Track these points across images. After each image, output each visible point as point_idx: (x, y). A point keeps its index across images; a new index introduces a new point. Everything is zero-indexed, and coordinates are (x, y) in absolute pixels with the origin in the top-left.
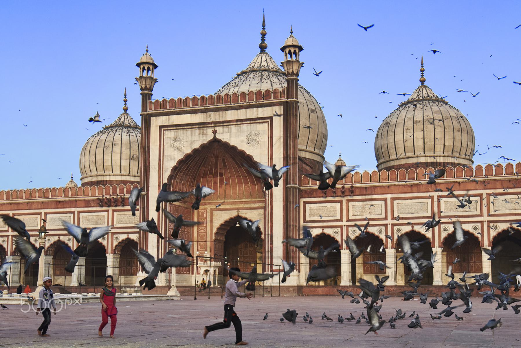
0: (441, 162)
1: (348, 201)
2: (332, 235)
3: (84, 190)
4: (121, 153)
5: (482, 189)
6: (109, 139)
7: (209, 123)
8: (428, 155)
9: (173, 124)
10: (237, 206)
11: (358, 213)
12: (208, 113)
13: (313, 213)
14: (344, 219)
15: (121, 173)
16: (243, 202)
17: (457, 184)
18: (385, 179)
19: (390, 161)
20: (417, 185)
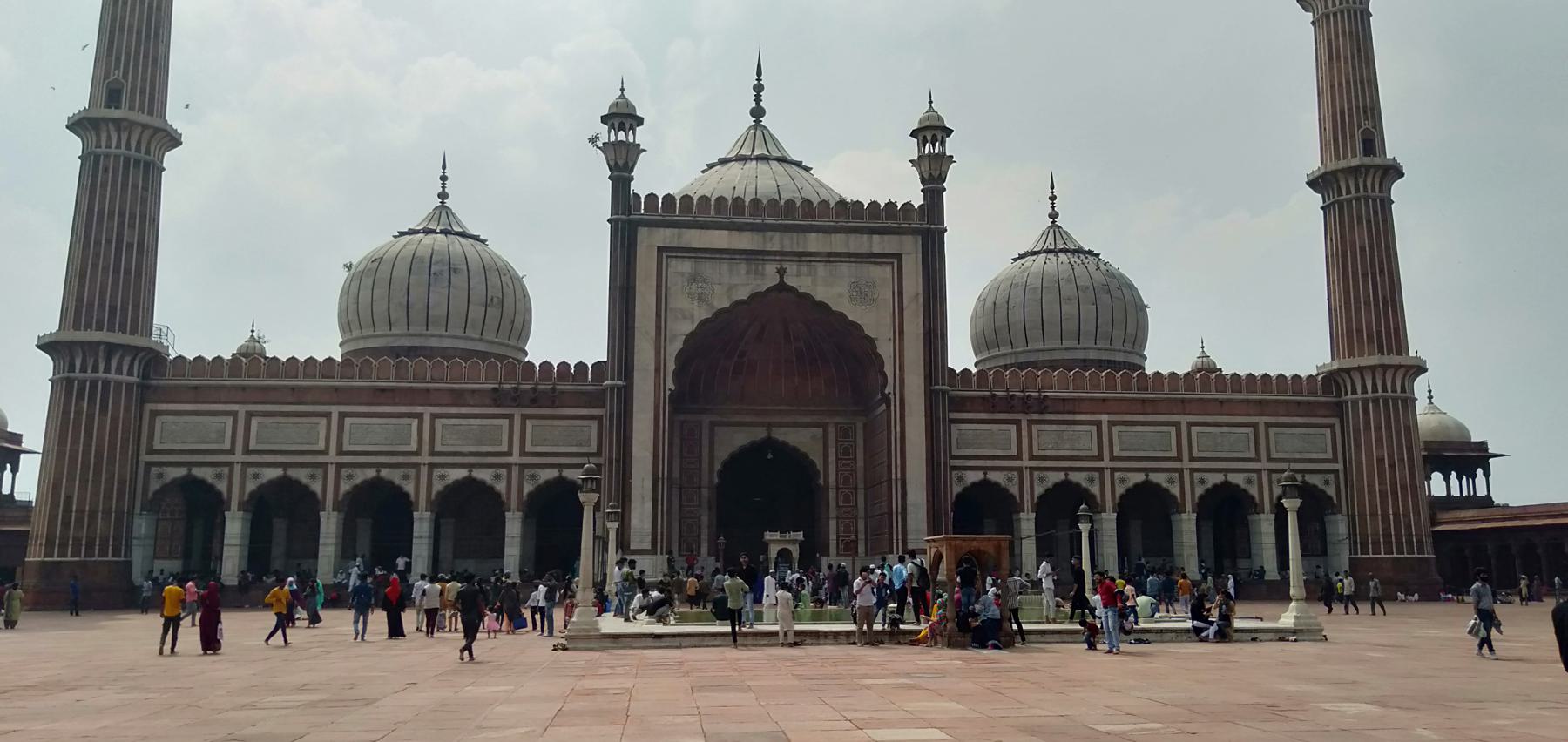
0: (1119, 362)
1: (1031, 422)
2: (1003, 484)
3: (447, 367)
8: (1104, 346)
10: (768, 419)
11: (1050, 446)
12: (770, 233)
14: (1025, 455)
16: (780, 410)
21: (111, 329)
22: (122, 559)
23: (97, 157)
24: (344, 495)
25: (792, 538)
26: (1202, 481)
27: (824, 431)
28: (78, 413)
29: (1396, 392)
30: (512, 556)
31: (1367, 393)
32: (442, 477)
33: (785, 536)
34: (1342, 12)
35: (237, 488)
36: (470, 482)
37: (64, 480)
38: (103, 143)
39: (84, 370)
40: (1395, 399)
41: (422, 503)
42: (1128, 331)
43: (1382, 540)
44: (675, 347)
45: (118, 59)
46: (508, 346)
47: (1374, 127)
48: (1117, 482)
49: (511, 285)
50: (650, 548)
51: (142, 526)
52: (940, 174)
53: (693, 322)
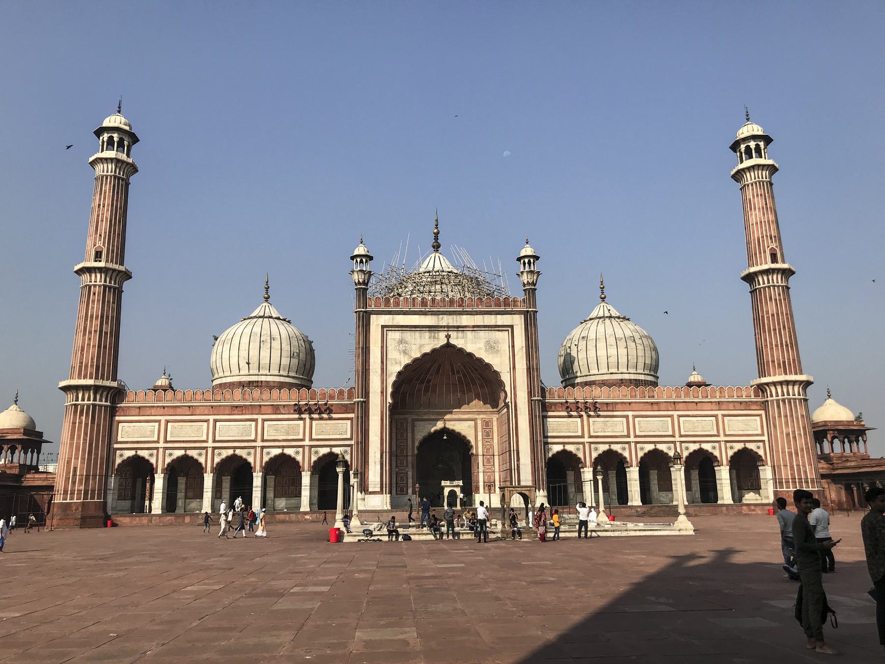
0: (642, 380)
1: (589, 416)
2: (574, 452)
4: (281, 350)
5: (717, 410)
6: (265, 333)
7: (441, 327)
9: (398, 324)
11: (600, 430)
12: (441, 316)
13: (552, 428)
14: (586, 435)
15: (279, 372)
17: (695, 404)
18: (625, 396)
19: (590, 375)
20: (657, 403)
21: (97, 378)
22: (102, 500)
23: (90, 287)
24: (217, 465)
25: (456, 484)
26: (687, 448)
27: (475, 423)
28: (80, 423)
29: (795, 395)
30: (305, 496)
31: (778, 396)
32: (268, 453)
33: (453, 483)
34: (756, 183)
35: (160, 461)
36: (283, 455)
37: (73, 459)
38: (93, 280)
39: (83, 400)
40: (795, 399)
41: (258, 468)
42: (646, 362)
43: (790, 480)
44: (392, 379)
45: (100, 235)
46: (302, 379)
47: (776, 247)
48: (638, 449)
49: (304, 345)
50: (379, 490)
51: (112, 482)
52: (533, 281)
53: (401, 365)
